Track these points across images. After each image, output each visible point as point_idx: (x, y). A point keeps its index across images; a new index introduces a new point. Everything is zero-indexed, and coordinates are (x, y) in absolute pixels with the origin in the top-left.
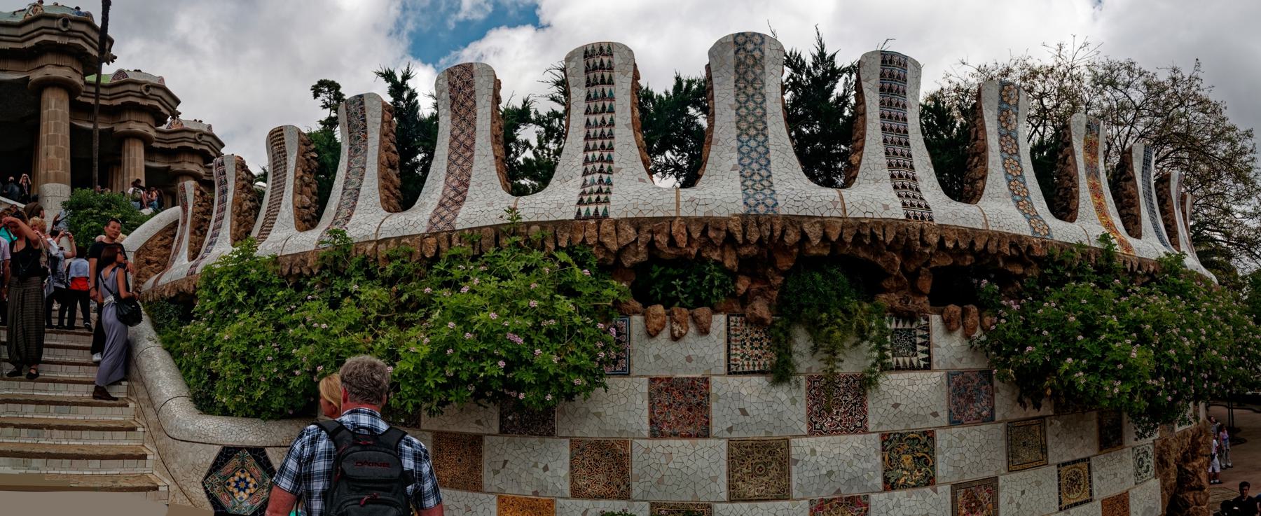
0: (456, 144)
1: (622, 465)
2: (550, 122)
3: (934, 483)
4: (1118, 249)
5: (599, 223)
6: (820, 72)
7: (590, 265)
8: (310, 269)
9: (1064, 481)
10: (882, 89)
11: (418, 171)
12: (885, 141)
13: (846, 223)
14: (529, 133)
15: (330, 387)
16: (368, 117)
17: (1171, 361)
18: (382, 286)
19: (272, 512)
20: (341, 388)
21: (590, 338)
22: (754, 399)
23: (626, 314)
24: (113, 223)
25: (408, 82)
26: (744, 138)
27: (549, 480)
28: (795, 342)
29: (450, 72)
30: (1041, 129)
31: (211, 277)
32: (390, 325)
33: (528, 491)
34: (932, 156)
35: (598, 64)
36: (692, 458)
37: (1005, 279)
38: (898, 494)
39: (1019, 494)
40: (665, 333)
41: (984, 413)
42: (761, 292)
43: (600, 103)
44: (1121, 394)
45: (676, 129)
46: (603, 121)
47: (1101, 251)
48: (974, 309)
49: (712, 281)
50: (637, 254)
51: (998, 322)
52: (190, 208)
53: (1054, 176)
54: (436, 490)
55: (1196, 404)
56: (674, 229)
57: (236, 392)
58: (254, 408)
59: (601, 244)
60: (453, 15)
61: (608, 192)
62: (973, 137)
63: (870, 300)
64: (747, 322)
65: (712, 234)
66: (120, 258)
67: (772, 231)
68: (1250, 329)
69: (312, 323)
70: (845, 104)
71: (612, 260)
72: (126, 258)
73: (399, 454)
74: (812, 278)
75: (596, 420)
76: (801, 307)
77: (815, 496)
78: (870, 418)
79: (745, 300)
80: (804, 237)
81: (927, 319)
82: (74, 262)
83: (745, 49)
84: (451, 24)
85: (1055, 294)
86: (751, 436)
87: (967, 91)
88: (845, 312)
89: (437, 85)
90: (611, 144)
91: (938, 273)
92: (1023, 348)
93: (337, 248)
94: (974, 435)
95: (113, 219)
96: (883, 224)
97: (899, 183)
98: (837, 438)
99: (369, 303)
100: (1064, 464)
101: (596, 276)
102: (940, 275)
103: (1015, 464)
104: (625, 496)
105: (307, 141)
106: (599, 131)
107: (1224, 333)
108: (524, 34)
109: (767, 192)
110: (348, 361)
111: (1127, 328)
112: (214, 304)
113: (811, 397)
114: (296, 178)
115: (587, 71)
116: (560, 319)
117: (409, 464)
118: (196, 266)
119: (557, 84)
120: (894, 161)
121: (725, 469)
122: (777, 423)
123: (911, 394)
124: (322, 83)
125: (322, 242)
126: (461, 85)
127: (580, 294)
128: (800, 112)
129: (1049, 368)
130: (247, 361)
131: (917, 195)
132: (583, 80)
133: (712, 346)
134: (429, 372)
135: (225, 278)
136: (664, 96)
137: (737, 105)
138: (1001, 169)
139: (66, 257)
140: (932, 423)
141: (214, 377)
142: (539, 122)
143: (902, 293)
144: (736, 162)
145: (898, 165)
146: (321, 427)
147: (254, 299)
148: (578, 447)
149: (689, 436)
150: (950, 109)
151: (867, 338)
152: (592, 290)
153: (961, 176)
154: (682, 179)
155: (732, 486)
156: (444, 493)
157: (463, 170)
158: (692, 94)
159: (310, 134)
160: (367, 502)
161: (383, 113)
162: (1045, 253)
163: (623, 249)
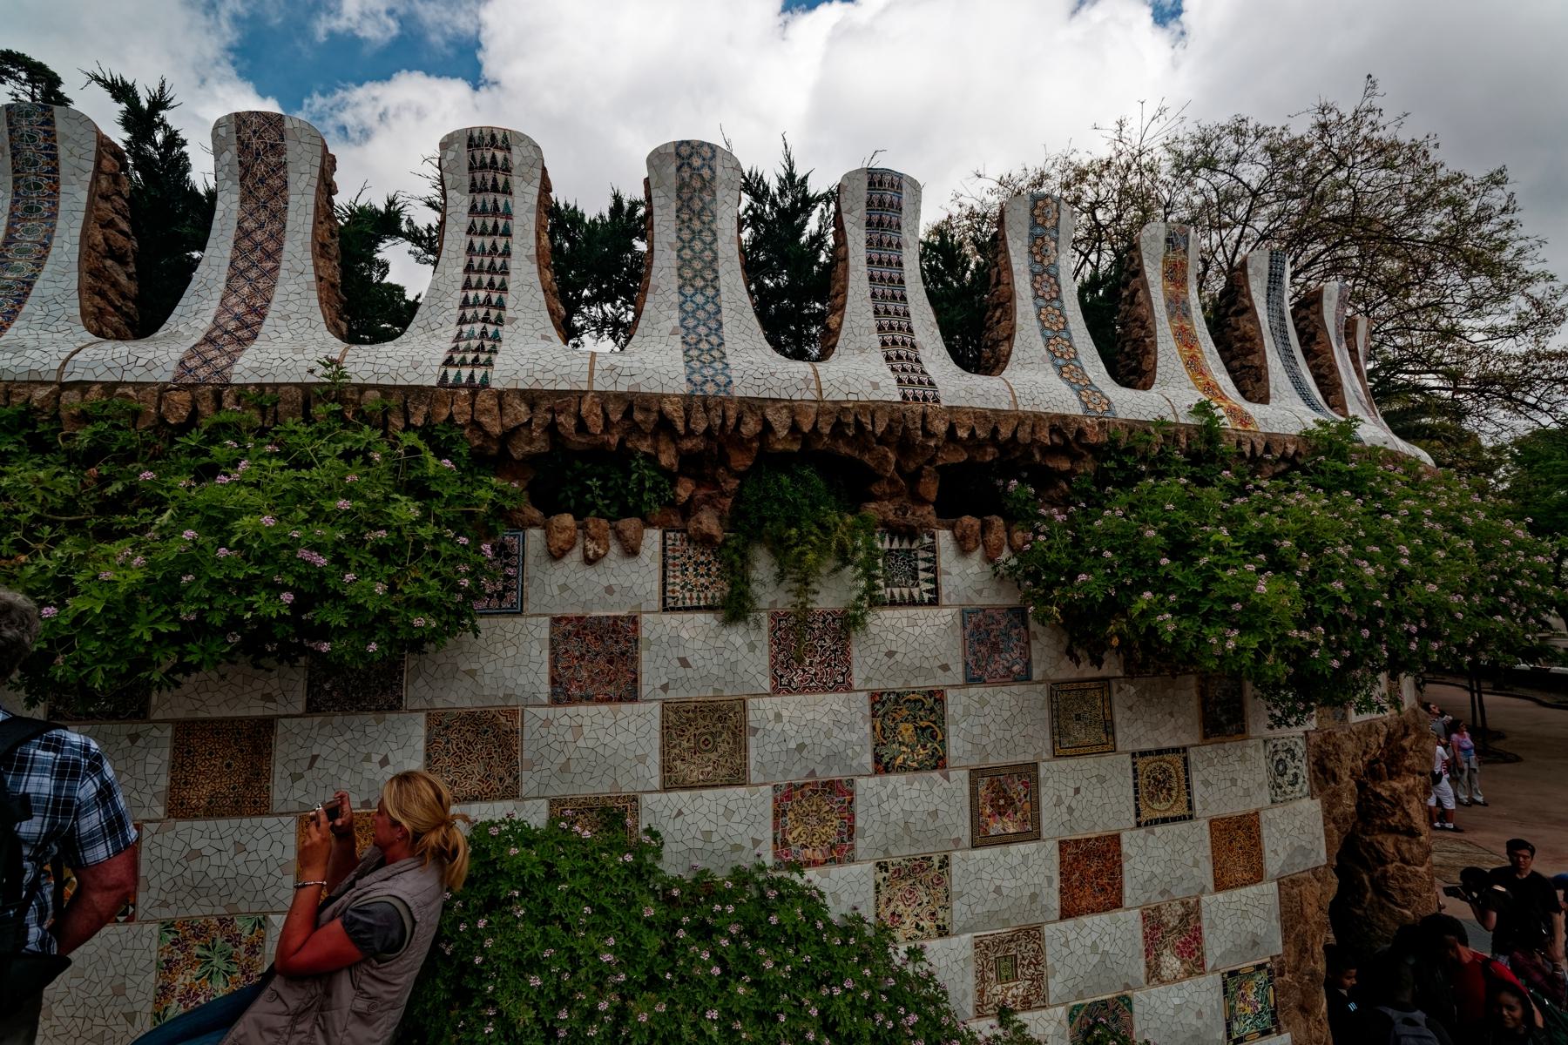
1: (508, 746)
3: (944, 766)
4: (1227, 423)
6: (788, 201)
9: (1143, 780)
10: (869, 224)
12: (874, 295)
17: (1337, 601)
22: (698, 644)
23: (519, 526)
28: (753, 567)
30: (1093, 257)
34: (937, 312)
37: (1043, 479)
38: (893, 779)
39: (1071, 792)
40: (576, 554)
41: (1016, 668)
44: (1239, 650)
47: (1197, 428)
48: (998, 522)
49: (641, 481)
50: (531, 441)
51: (1035, 539)
53: (1117, 326)
55: (1393, 677)
59: (476, 425)
61: (494, 351)
62: (993, 281)
68: (1519, 544)
70: (821, 246)
71: (494, 449)
75: (468, 681)
77: (781, 780)
78: (855, 671)
79: (687, 510)
81: (933, 536)
83: (690, 165)
85: (1123, 497)
87: (985, 216)
90: (503, 283)
91: (946, 473)
92: (1072, 576)
94: (1002, 700)
97: (893, 353)
98: (811, 698)
100: (1143, 754)
102: (948, 475)
103: (1063, 747)
106: (487, 261)
107: (1453, 554)
109: (718, 365)
111: (1246, 547)
113: (775, 641)
120: (885, 322)
122: (729, 678)
123: (913, 638)
127: (438, 495)
128: (762, 258)
129: (1114, 607)
131: (917, 367)
133: (644, 571)
137: (679, 244)
138: (1035, 322)
140: (940, 680)
143: (898, 501)
145: (891, 328)
148: (440, 725)
150: (961, 245)
151: (849, 562)
152: (455, 490)
153: (976, 331)
162: (1103, 438)
163: (510, 434)
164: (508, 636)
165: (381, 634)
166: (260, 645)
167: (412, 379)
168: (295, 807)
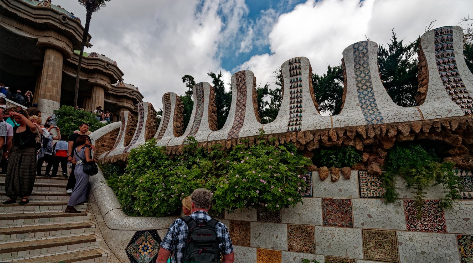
0: (239, 103)
2: (276, 93)
5: (297, 133)
7: (294, 151)
8: (179, 152)
11: (224, 114)
13: (424, 123)
14: (267, 98)
15: (187, 202)
16: (204, 92)
18: (209, 160)
19: (159, 260)
20: (191, 202)
21: (295, 181)
23: (310, 171)
24: (84, 125)
25: (220, 78)
26: (361, 91)
27: (279, 242)
29: (237, 74)
31: (134, 155)
32: (212, 176)
33: (270, 247)
35: (295, 67)
36: (344, 236)
40: (329, 179)
42: (375, 160)
43: (296, 83)
45: (329, 90)
46: (298, 91)
49: (350, 155)
50: (314, 145)
52: (126, 123)
54: (231, 246)
56: (330, 134)
57: (144, 205)
58: (152, 212)
59: (298, 142)
60: (238, 51)
61: (301, 120)
63: (441, 161)
64: (368, 174)
65: (349, 134)
66: (87, 142)
67: (381, 131)
69: (180, 175)
71: (303, 148)
72: (91, 143)
73: (215, 230)
74: (404, 152)
75: (298, 216)
76: (399, 166)
79: (367, 164)
80: (399, 132)
82: (59, 142)
84: (237, 55)
86: (374, 228)
88: (427, 168)
89: (231, 79)
90: (301, 100)
93: (191, 144)
95: (84, 123)
96: (450, 121)
99: (204, 167)
101: (296, 155)
104: (313, 251)
105: (179, 99)
106: (296, 95)
108: (265, 58)
110: (195, 191)
112: (136, 166)
114: (174, 115)
115: (290, 71)
116: (282, 173)
117: (219, 234)
118: (127, 149)
119: (278, 77)
121: (361, 243)
124: (186, 76)
125: (185, 142)
126: (241, 79)
127: (290, 163)
130: (150, 191)
132: (289, 74)
134: (228, 195)
135: (141, 155)
136: (323, 76)
139: (54, 139)
141: (134, 199)
142: (271, 93)
144: (358, 102)
146: (183, 219)
147: (154, 165)
148: (291, 228)
149: (342, 226)
154: (333, 111)
155: (365, 252)
156: (234, 247)
157: (242, 114)
158: (337, 73)
159: (181, 97)
160: (202, 252)
161: (211, 90)
163: (308, 144)
164: (309, 204)
165: (279, 203)
166: (250, 203)
167: (280, 131)
168: (256, 246)
